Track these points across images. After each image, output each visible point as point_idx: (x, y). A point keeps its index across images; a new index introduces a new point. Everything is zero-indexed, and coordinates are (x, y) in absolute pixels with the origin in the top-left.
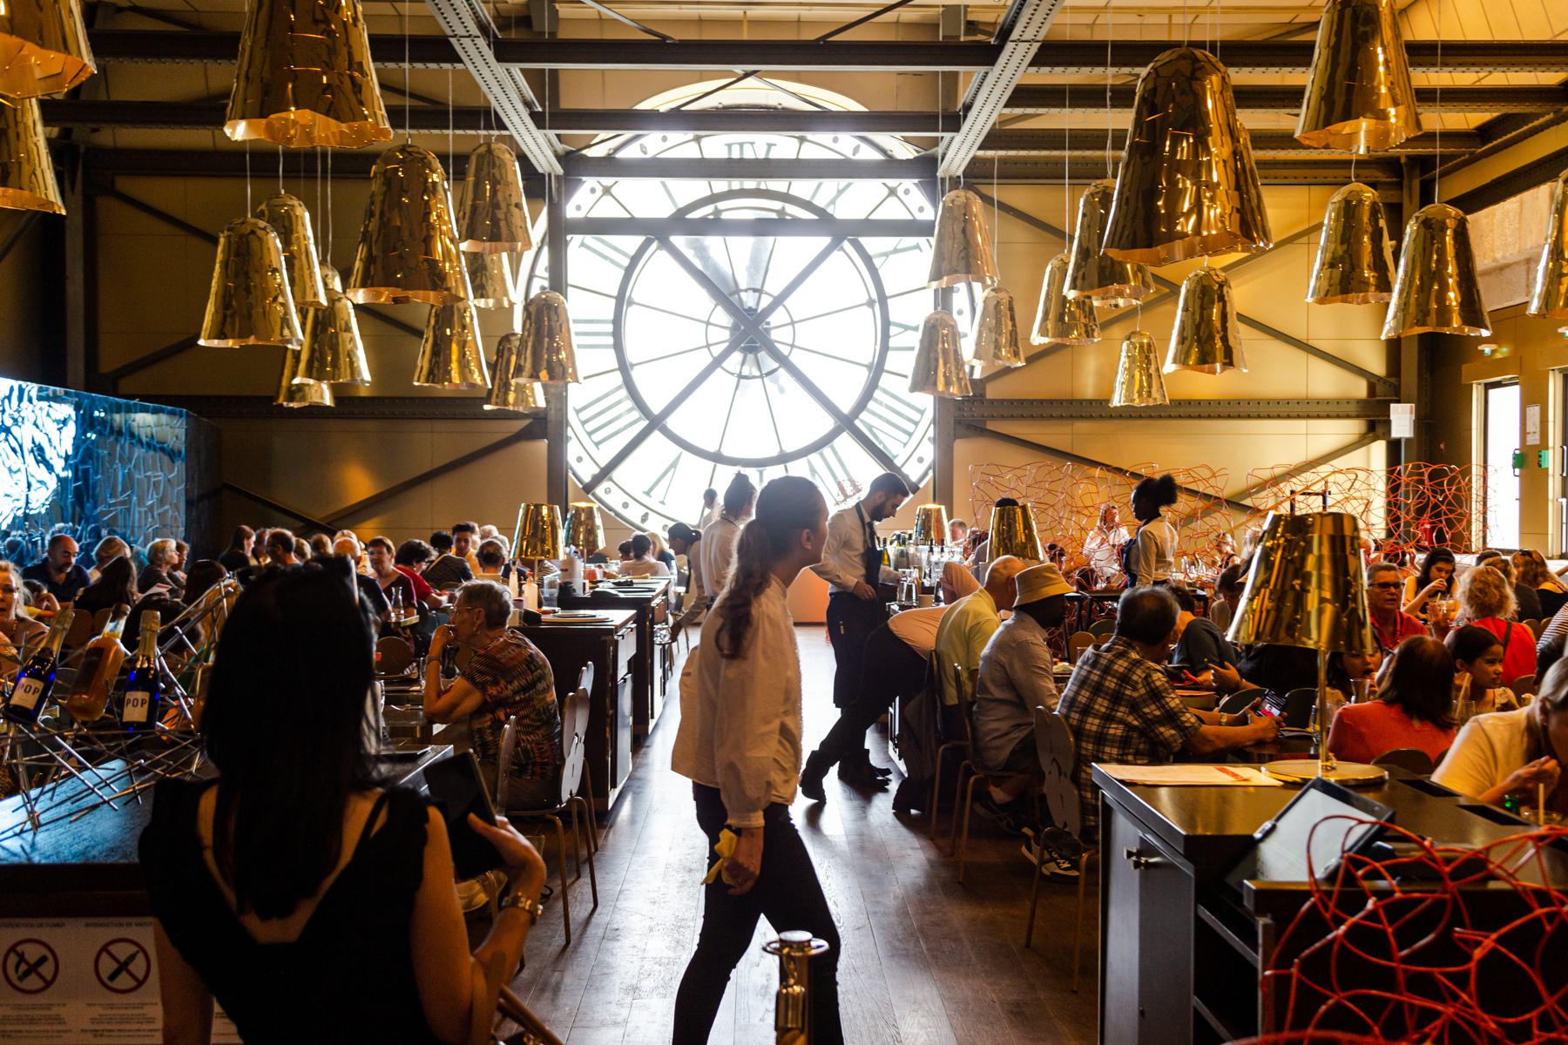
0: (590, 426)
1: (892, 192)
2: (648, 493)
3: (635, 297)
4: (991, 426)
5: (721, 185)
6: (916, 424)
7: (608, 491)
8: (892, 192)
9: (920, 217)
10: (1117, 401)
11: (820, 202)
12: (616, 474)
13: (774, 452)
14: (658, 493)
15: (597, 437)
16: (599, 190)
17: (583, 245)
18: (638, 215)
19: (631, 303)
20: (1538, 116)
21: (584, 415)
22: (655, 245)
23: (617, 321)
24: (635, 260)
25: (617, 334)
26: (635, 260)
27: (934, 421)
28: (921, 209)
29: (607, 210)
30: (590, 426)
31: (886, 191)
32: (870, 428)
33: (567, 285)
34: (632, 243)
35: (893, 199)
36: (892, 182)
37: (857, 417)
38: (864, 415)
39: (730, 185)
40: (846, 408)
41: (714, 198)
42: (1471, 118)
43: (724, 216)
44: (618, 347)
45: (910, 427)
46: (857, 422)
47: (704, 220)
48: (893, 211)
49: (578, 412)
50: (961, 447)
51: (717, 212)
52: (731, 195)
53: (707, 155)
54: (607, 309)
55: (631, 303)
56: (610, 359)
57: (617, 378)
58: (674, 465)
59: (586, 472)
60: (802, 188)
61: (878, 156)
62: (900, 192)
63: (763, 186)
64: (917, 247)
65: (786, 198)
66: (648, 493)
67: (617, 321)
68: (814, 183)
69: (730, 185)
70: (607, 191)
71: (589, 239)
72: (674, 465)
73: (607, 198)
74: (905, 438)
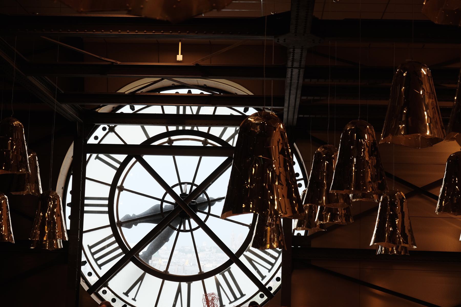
0: (96, 256)
2: (126, 294)
3: (125, 186)
5: (172, 128)
6: (276, 259)
7: (104, 292)
11: (224, 138)
12: (111, 284)
13: (196, 272)
14: (132, 294)
15: (100, 262)
16: (108, 128)
17: (97, 158)
18: (128, 143)
19: (121, 189)
21: (93, 250)
22: (134, 160)
23: (111, 198)
24: (124, 165)
25: (110, 205)
26: (124, 165)
27: (282, 265)
29: (111, 139)
30: (96, 256)
32: (250, 260)
33: (85, 178)
34: (121, 158)
38: (247, 253)
39: (167, 129)
40: (234, 249)
41: (168, 134)
43: (175, 144)
44: (111, 213)
45: (273, 261)
46: (242, 259)
47: (160, 146)
49: (90, 248)
51: (171, 141)
52: (177, 133)
54: (105, 192)
55: (121, 189)
56: (105, 219)
57: (109, 231)
58: (141, 278)
59: (93, 280)
60: (216, 131)
63: (195, 129)
65: (207, 136)
66: (126, 294)
67: (111, 198)
68: (221, 129)
69: (177, 128)
70: (112, 130)
71: (101, 156)
72: (141, 278)
73: (112, 135)
74: (269, 267)
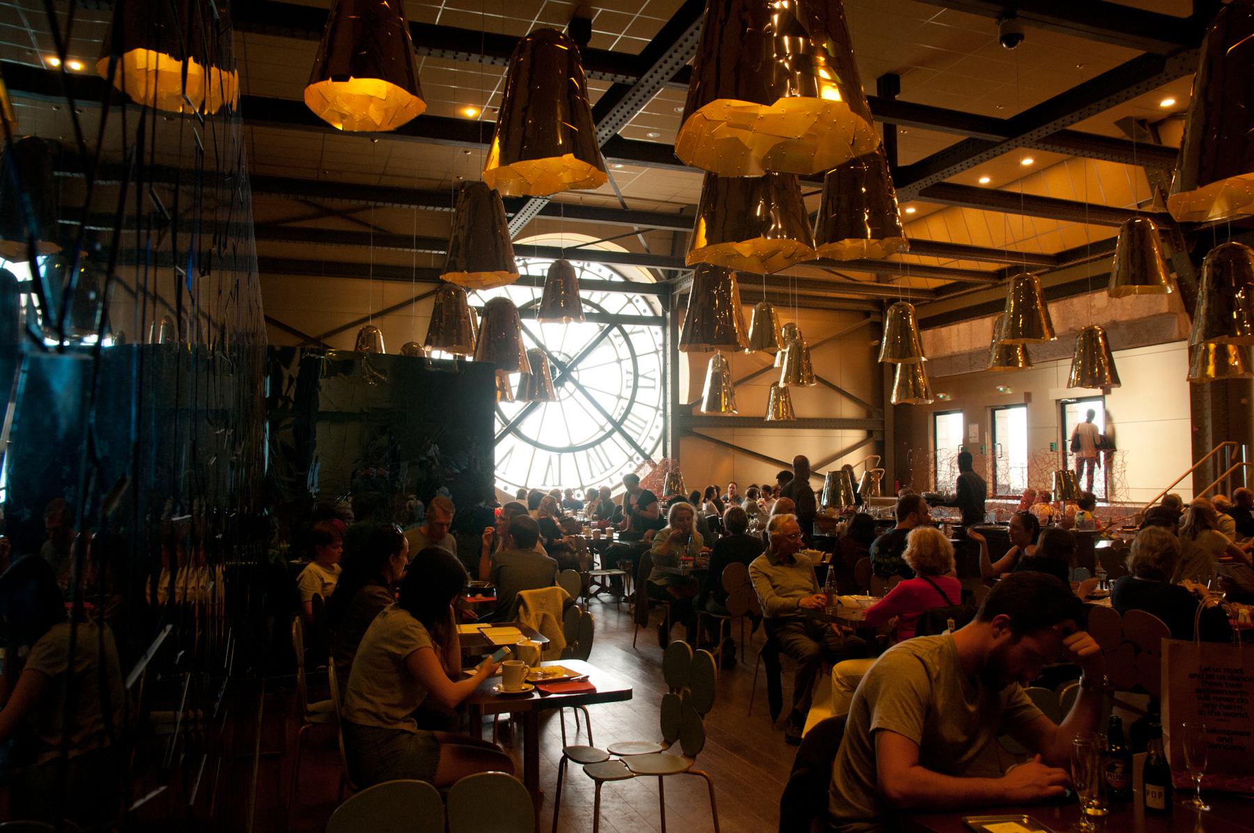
1: (630, 301)
4: (695, 430)
8: (630, 301)
9: (644, 314)
10: (770, 417)
20: (981, 284)
28: (645, 311)
31: (626, 300)
35: (630, 305)
36: (630, 295)
37: (622, 424)
38: (626, 422)
42: (934, 283)
48: (630, 311)
50: (685, 444)
53: (530, 274)
61: (621, 280)
62: (634, 300)
64: (643, 331)
